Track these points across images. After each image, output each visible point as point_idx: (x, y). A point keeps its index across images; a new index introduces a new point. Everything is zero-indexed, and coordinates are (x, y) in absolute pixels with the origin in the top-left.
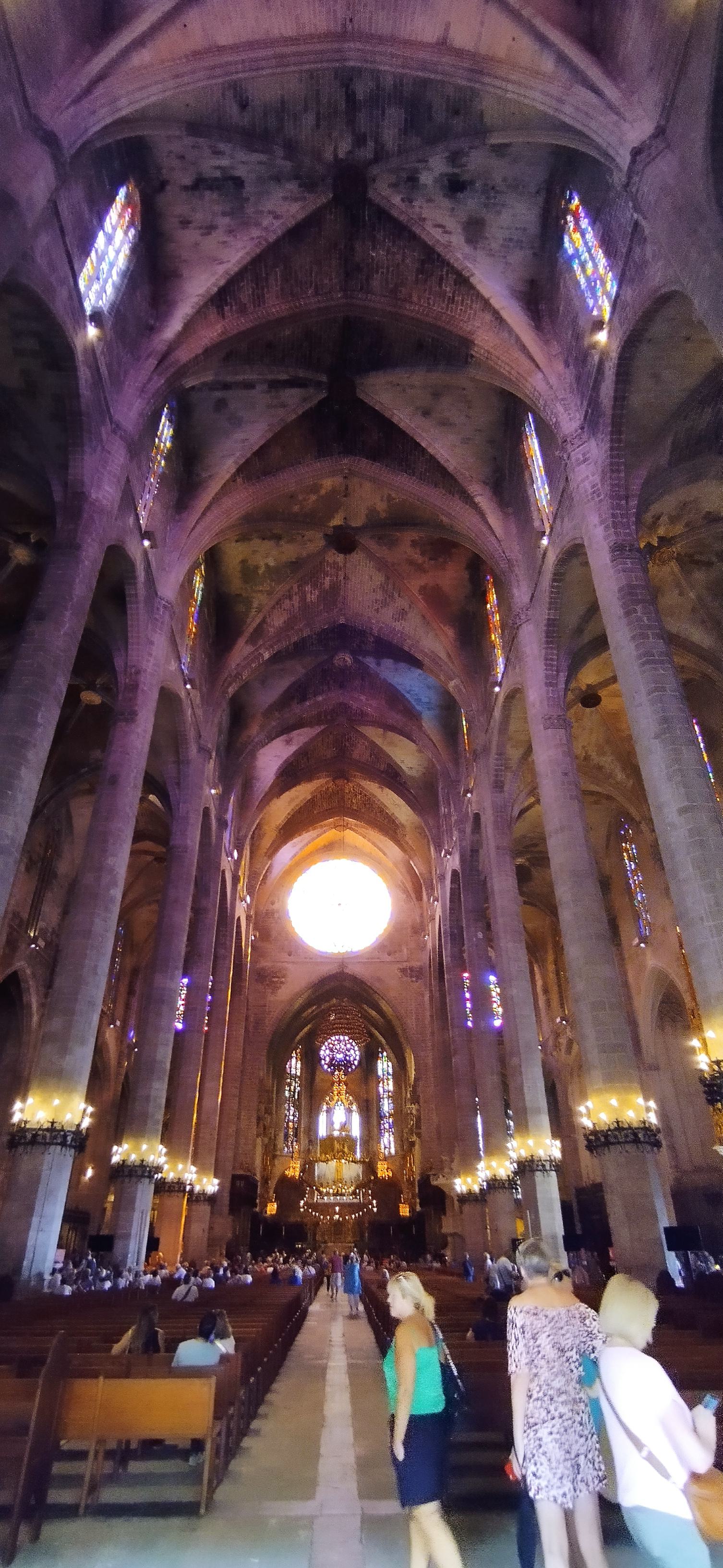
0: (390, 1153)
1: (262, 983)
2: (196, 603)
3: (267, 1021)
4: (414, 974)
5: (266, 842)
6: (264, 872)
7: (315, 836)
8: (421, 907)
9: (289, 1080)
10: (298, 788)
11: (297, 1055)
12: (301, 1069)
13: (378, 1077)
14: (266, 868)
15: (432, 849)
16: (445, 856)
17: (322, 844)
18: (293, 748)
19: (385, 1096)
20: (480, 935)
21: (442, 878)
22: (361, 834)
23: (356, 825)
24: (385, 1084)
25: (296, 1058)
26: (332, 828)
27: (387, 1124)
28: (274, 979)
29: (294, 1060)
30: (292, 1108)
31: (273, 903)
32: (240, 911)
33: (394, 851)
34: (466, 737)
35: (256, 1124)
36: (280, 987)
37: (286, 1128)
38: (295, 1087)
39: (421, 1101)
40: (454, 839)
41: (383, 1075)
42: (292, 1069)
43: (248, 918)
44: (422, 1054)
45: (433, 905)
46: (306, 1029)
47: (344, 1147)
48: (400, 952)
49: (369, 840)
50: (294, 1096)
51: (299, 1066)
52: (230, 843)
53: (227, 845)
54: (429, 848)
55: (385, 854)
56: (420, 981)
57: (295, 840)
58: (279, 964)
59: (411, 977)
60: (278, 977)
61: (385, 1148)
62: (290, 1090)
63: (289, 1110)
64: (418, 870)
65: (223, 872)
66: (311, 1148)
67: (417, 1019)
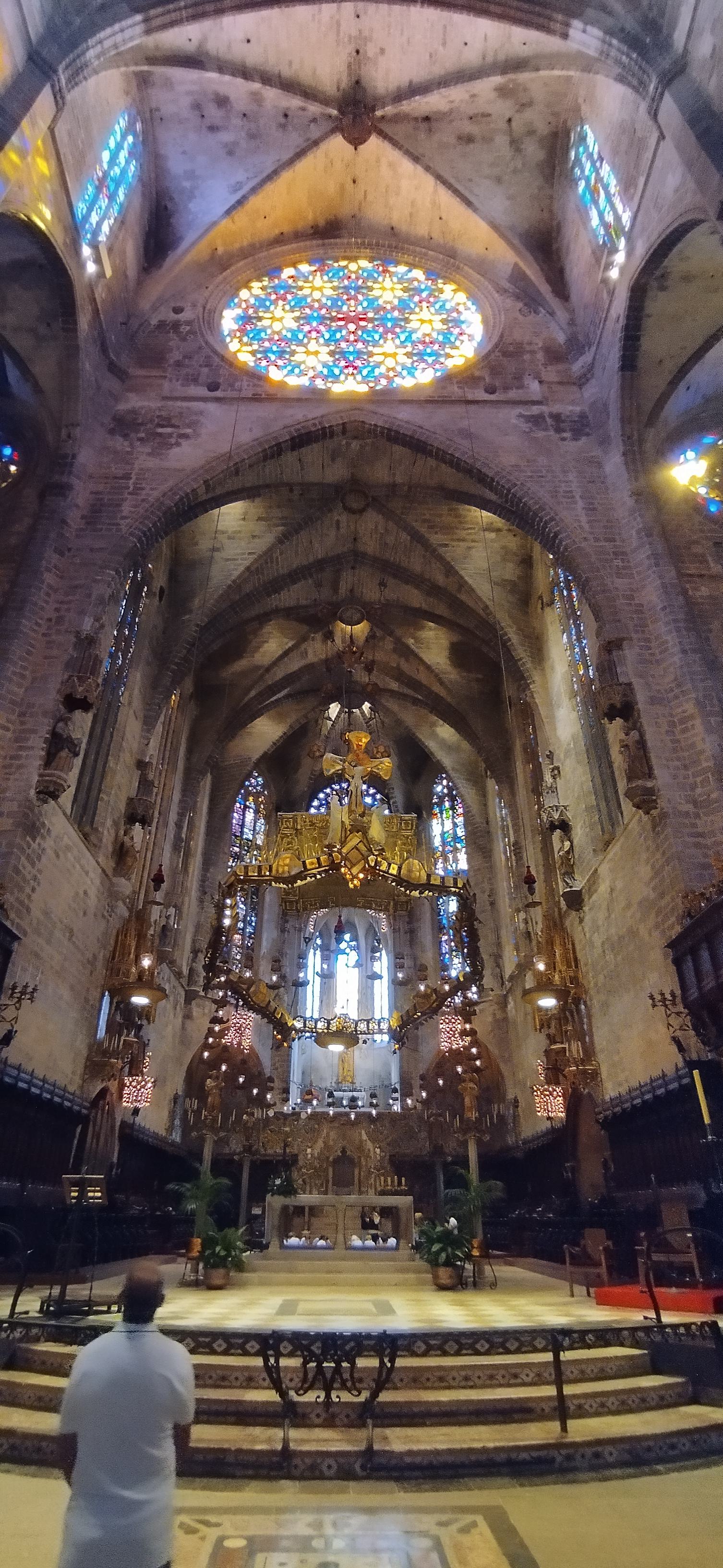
1: (125, 436)
3: (126, 509)
4: (562, 425)
9: (237, 849)
12: (268, 834)
13: (432, 850)
25: (257, 812)
28: (160, 430)
29: (250, 816)
30: (242, 906)
31: (178, 310)
39: (641, 698)
44: (620, 583)
48: (518, 388)
49: (428, 169)
55: (468, 203)
56: (584, 439)
59: (558, 430)
60: (173, 426)
67: (591, 509)
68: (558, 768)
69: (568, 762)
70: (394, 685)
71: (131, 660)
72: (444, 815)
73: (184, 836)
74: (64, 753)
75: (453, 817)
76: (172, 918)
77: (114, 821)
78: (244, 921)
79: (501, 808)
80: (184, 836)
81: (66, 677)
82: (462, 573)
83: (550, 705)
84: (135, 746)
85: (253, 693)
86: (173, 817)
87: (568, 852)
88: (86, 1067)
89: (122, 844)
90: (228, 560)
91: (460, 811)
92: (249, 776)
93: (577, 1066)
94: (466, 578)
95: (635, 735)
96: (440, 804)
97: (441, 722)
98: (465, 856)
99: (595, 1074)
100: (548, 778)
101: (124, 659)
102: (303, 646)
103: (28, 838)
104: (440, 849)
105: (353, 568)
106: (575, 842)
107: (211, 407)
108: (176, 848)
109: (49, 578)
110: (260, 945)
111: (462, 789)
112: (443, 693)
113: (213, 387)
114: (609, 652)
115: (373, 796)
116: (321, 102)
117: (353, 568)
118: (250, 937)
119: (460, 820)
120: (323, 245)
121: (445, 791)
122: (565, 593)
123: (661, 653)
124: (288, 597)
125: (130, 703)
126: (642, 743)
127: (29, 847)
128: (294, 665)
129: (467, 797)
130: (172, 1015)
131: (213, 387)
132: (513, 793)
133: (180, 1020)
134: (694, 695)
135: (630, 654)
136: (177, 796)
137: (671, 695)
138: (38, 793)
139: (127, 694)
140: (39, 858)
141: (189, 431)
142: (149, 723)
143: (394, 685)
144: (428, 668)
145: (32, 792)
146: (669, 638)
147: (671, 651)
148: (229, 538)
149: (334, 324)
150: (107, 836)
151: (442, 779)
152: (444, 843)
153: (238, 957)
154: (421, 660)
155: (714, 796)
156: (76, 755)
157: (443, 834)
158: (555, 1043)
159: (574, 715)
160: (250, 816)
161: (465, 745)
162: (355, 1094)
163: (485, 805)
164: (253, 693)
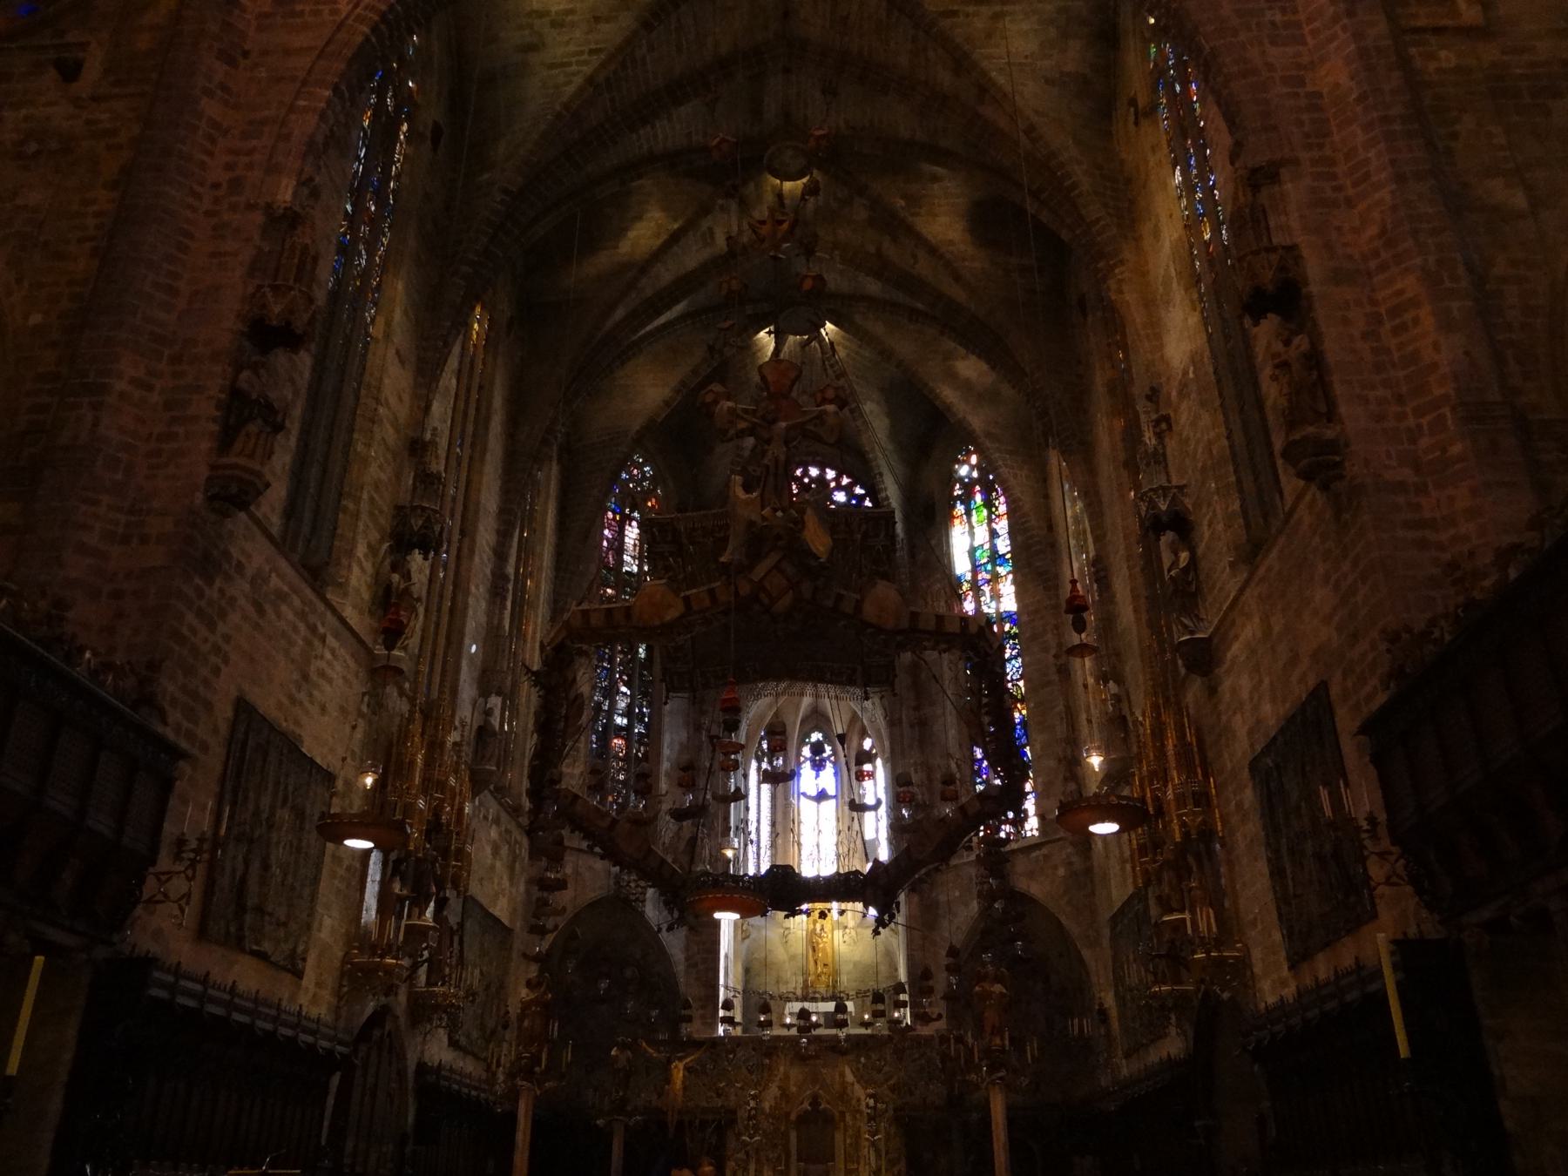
13: (958, 582)
24: (986, 599)
30: (624, 689)
35: (215, 428)
39: (1314, 269)
63: (611, 693)
68: (1167, 419)
69: (1184, 406)
70: (873, 287)
71: (384, 259)
72: (974, 518)
73: (510, 570)
74: (252, 428)
75: (990, 521)
76: (497, 712)
77: (369, 546)
78: (628, 713)
79: (1074, 500)
80: (510, 570)
81: (251, 290)
82: (985, 64)
83: (1150, 304)
84: (403, 412)
85: (620, 313)
86: (486, 536)
87: (1186, 570)
88: (342, 974)
89: (388, 587)
90: (552, 66)
91: (1003, 509)
92: (624, 463)
93: (1208, 952)
94: (994, 74)
95: (1301, 342)
96: (967, 499)
97: (962, 351)
98: (1013, 588)
99: (1244, 963)
100: (1149, 438)
101: (371, 256)
102: (705, 224)
103: (198, 581)
104: (969, 576)
105: (787, 71)
106: (1200, 551)
108: (497, 592)
109: (211, 108)
110: (659, 754)
111: (1003, 470)
112: (958, 294)
114: (1255, 188)
115: (848, 489)
117: (787, 71)
118: (640, 743)
119: (1002, 526)
121: (975, 474)
122: (1178, 88)
123: (1355, 184)
124: (671, 130)
125: (388, 336)
126: (1314, 359)
127: (201, 595)
128: (691, 257)
129: (1012, 482)
130: (506, 883)
132: (1092, 472)
133: (522, 888)
134: (1418, 261)
135: (1294, 189)
136: (490, 499)
137: (1373, 264)
138: (211, 499)
139: (380, 321)
140: (223, 614)
142: (426, 372)
143: (873, 287)
144: (933, 251)
145: (199, 498)
146: (1372, 154)
147: (1375, 179)
148: (554, 24)
150: (358, 577)
151: (969, 453)
152: (975, 569)
154: (919, 238)
155: (1456, 449)
156: (279, 428)
157: (972, 551)
158: (1171, 911)
159: (1194, 319)
161: (1007, 391)
162: (807, 1005)
163: (1047, 497)
164: (620, 313)
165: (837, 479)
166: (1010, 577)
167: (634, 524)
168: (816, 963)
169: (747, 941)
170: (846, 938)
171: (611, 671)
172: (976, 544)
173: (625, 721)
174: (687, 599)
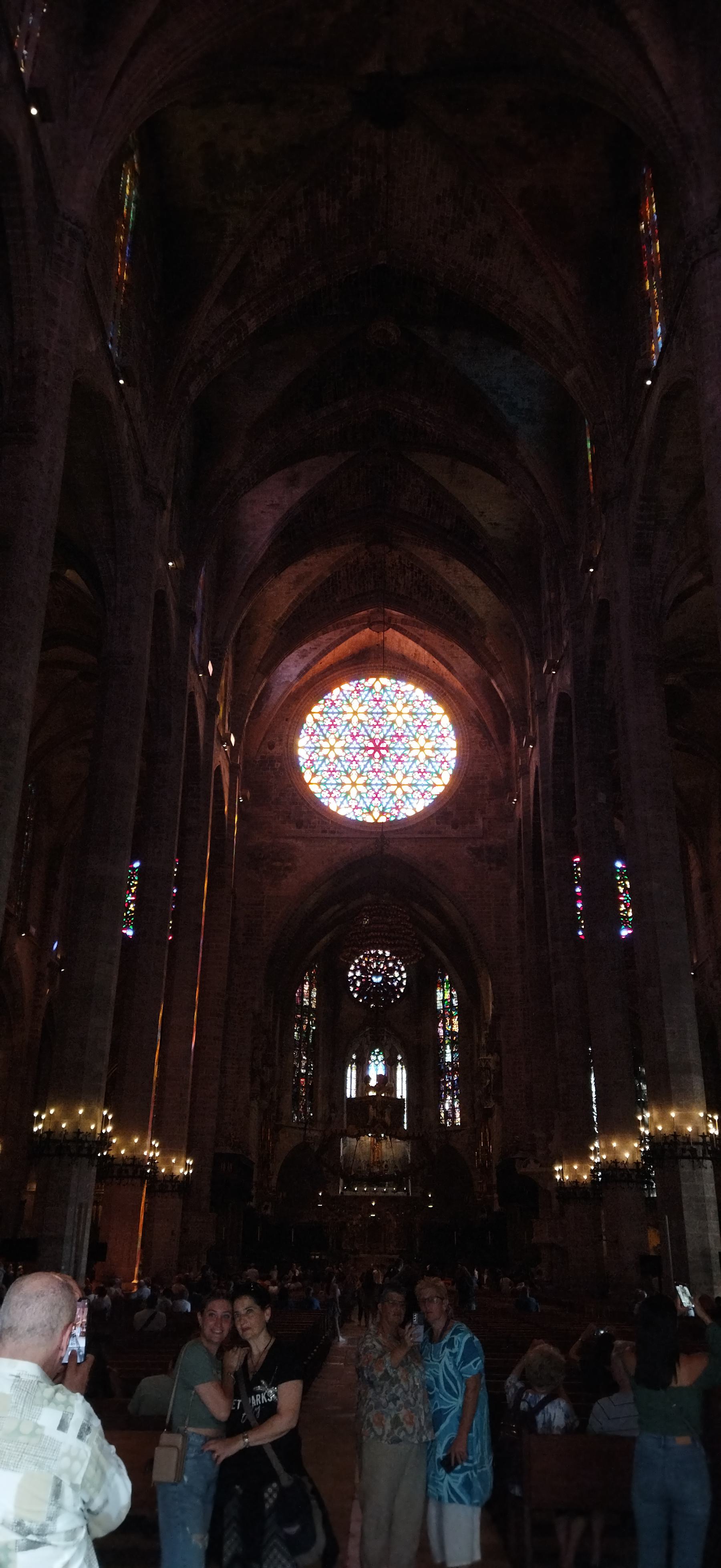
0: (453, 1124)
2: (127, 225)
5: (260, 649)
6: (256, 697)
7: (338, 637)
8: (509, 754)
10: (310, 559)
11: (310, 976)
14: (259, 692)
15: (527, 661)
16: (548, 671)
17: (350, 652)
18: (299, 492)
19: (447, 1042)
20: (602, 798)
21: (542, 706)
22: (412, 637)
23: (403, 621)
24: (448, 1023)
26: (365, 627)
27: (450, 1083)
29: (306, 987)
30: (304, 1058)
31: (271, 747)
32: (221, 759)
33: (467, 663)
34: (591, 471)
35: (249, 1080)
36: (286, 876)
37: (294, 1086)
38: (308, 1025)
40: (565, 643)
41: (444, 1008)
42: (305, 1000)
43: (233, 769)
45: (527, 751)
46: (324, 940)
47: (382, 1114)
49: (425, 646)
50: (307, 1039)
51: (314, 995)
52: (200, 647)
53: (196, 653)
54: (523, 663)
55: (450, 668)
57: (304, 647)
58: (282, 841)
61: (447, 1116)
62: (300, 1031)
64: (504, 695)
65: (192, 695)
66: (333, 1115)
72: (445, 986)
78: (306, 1067)
107: (299, 843)
113: (299, 825)
116: (357, 623)
118: (310, 1079)
120: (358, 668)
131: (299, 825)
141: (290, 864)
149: (366, 754)
153: (304, 1094)
157: (443, 1001)
160: (306, 987)
165: (390, 956)
166: (457, 1017)
167: (307, 983)
168: (374, 1157)
169: (345, 1148)
170: (387, 1146)
171: (299, 1052)
172: (446, 998)
173: (305, 1071)
174: (359, 1131)
